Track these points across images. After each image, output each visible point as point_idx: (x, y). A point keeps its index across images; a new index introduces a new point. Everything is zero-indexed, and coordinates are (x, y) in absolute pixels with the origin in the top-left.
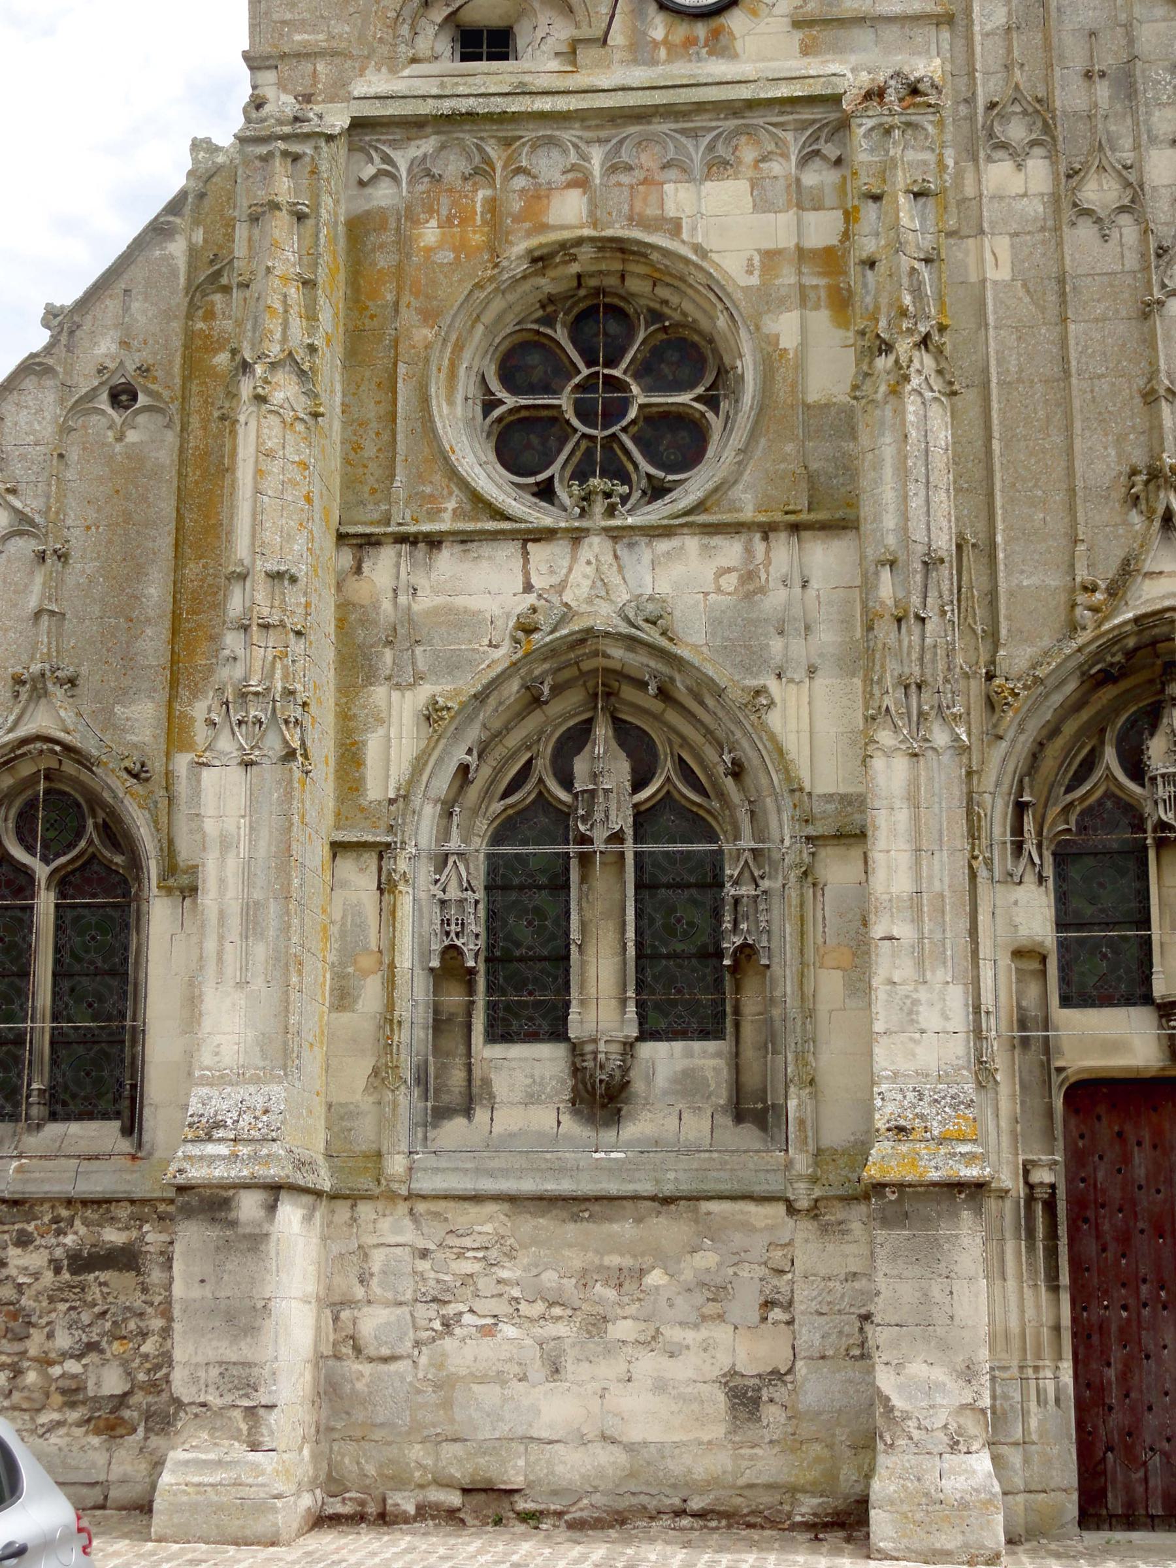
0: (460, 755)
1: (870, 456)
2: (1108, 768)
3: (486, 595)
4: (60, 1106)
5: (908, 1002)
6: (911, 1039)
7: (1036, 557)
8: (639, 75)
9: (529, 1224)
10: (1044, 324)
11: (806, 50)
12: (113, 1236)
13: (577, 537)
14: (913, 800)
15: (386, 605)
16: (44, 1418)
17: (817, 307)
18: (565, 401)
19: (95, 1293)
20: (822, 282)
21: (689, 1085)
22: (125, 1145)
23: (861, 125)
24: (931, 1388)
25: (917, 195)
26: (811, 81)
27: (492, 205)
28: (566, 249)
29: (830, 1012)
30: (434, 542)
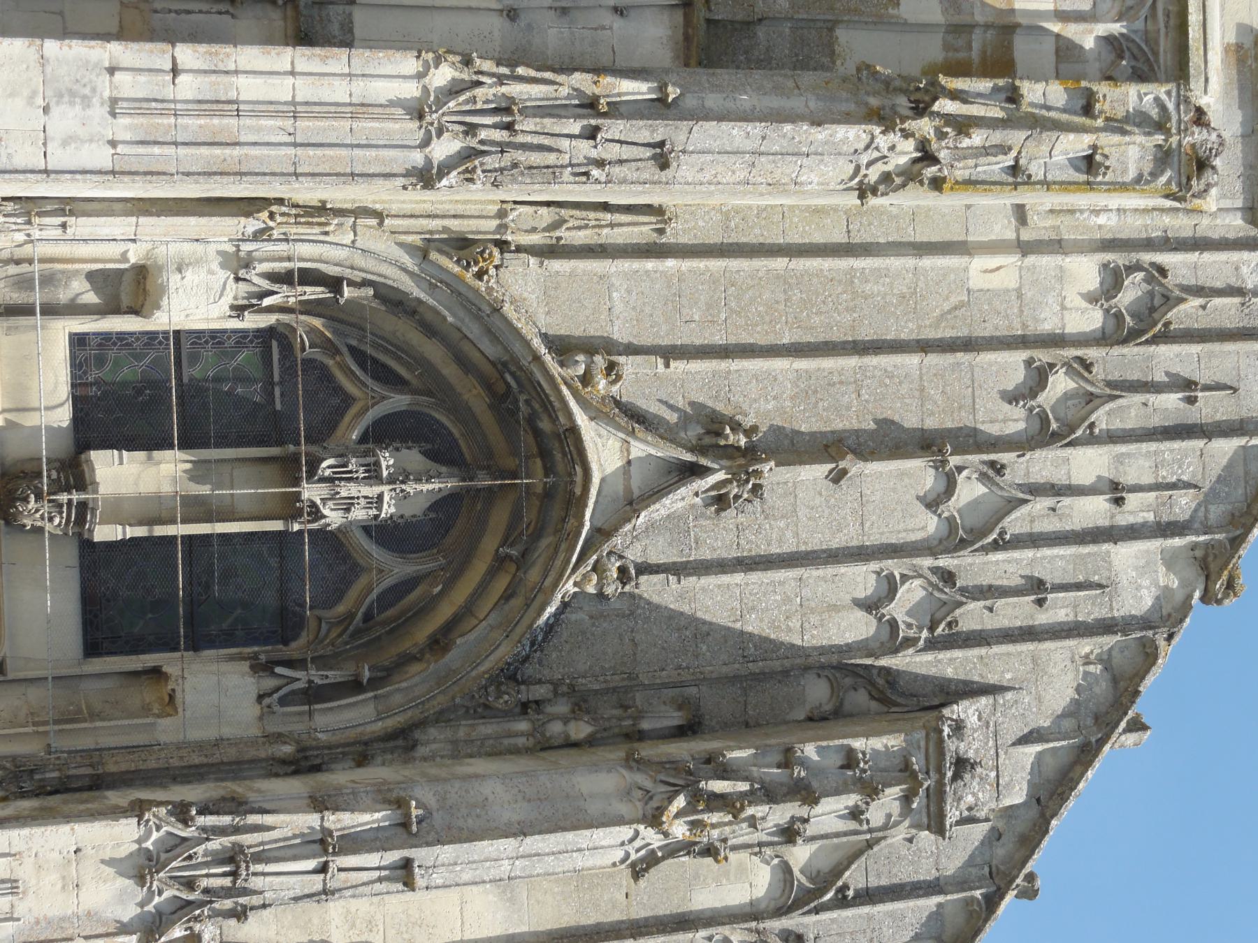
1: (790, 84)
2: (384, 398)
5: (87, 91)
6: (34, 94)
7: (648, 310)
10: (919, 327)
17: (947, 47)
20: (975, 54)
23: (1168, 93)
25: (1089, 159)
26: (1202, 53)
29: (61, 14)
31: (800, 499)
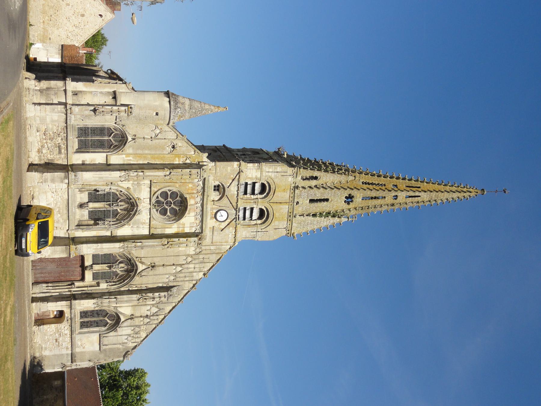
0: (123, 191)
3: (143, 196)
4: (80, 142)
8: (209, 209)
9: (66, 202)
11: (210, 228)
12: (63, 151)
13: (150, 204)
14: (114, 248)
15: (143, 182)
16: (39, 143)
18: (169, 199)
19: (56, 149)
21: (83, 216)
22: (75, 150)
24: (47, 252)
27: (193, 193)
28: (187, 201)
30: (150, 188)
31: (160, 270)
